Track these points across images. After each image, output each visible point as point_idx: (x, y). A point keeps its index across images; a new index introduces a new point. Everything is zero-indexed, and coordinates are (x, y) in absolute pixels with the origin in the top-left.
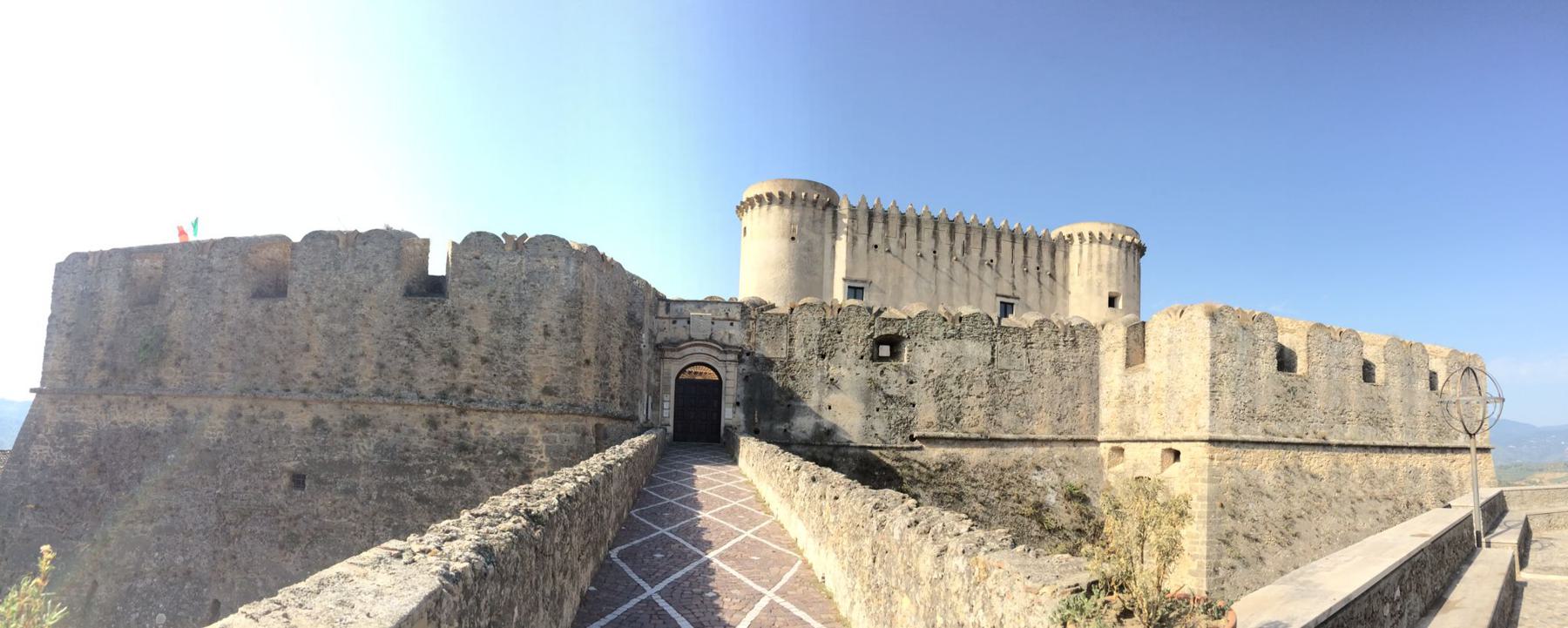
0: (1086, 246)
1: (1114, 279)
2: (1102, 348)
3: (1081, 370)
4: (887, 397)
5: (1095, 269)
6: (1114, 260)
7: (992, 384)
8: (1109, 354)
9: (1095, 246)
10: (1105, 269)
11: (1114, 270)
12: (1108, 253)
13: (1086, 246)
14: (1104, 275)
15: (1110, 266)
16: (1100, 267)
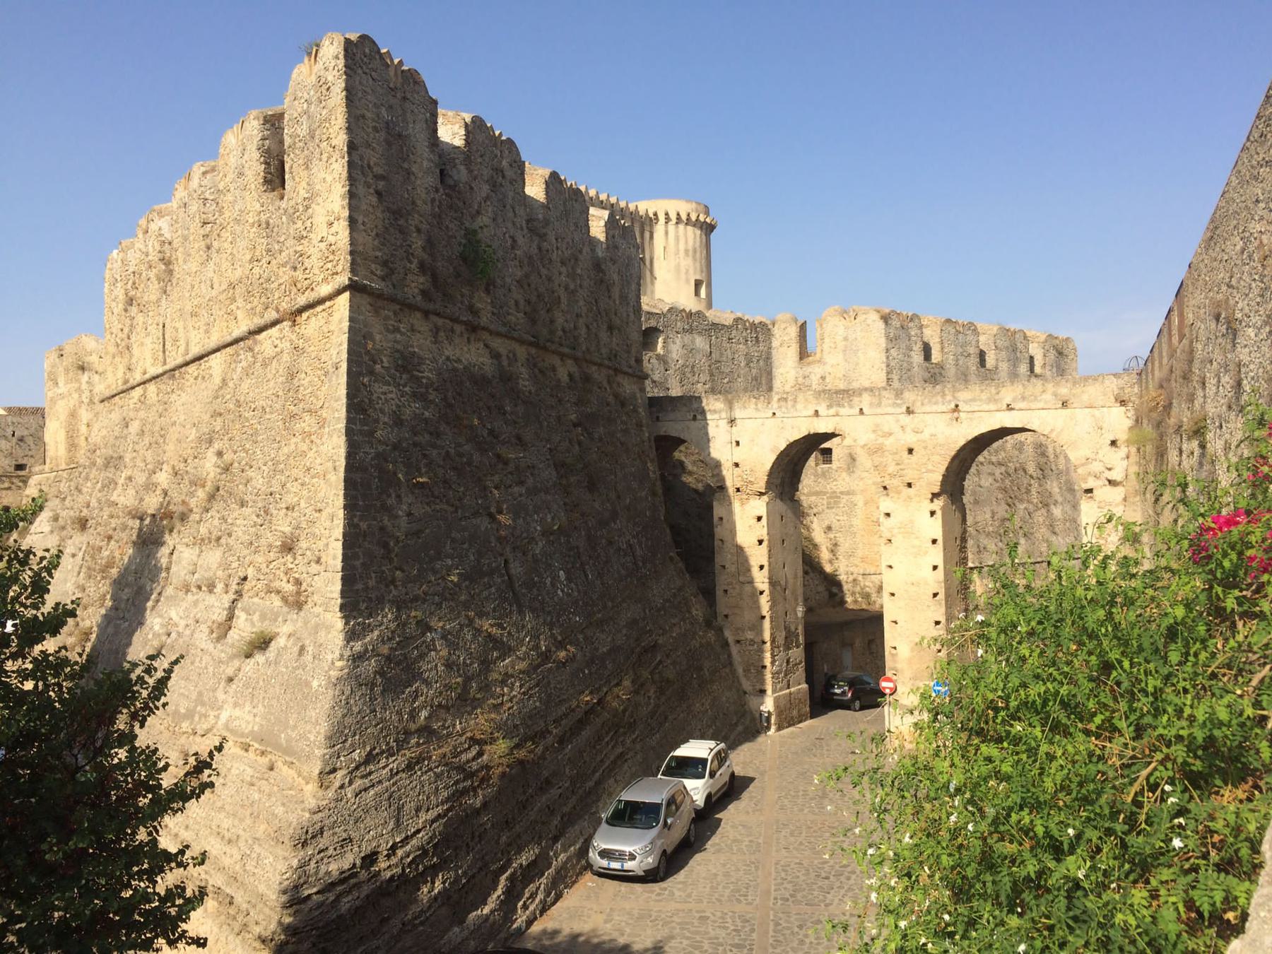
0: (671, 227)
1: (698, 265)
2: (774, 345)
3: (761, 363)
4: (654, 382)
5: (682, 253)
6: (698, 244)
7: (712, 375)
8: (781, 350)
9: (681, 227)
10: (691, 253)
11: (698, 255)
12: (692, 236)
13: (671, 227)
14: (689, 261)
15: (695, 251)
16: (686, 251)
